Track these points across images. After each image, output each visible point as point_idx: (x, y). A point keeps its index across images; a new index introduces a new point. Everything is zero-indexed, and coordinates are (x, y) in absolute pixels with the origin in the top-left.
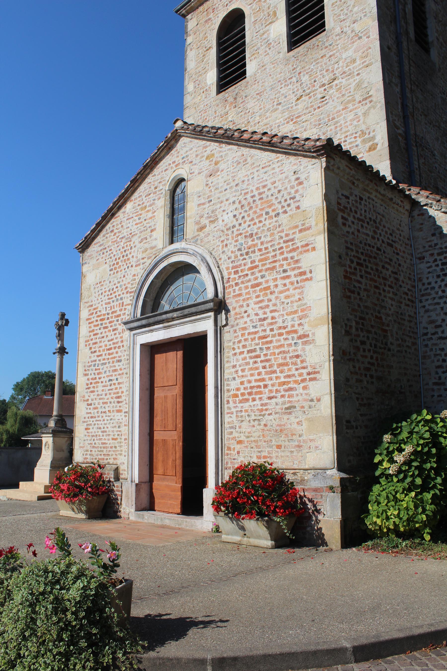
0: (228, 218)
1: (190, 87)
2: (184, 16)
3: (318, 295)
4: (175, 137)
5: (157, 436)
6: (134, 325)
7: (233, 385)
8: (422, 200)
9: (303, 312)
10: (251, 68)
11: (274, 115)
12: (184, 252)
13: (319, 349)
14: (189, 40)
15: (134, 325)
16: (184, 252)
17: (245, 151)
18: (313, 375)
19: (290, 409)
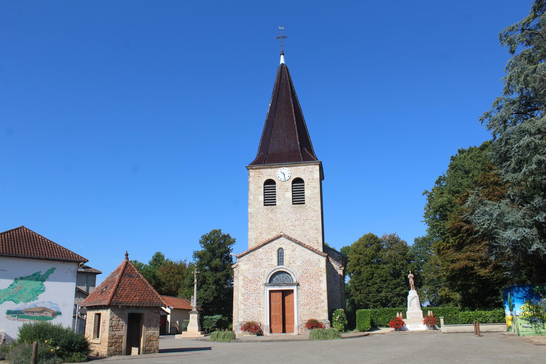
0: (299, 263)
1: (251, 197)
2: (248, 169)
3: (324, 286)
4: (281, 236)
5: (272, 314)
6: (266, 285)
7: (301, 303)
8: (330, 260)
9: (321, 289)
10: (278, 203)
11: (287, 222)
12: (283, 268)
13: (324, 296)
14: (250, 179)
15: (266, 285)
16: (283, 268)
17: (303, 248)
18: (323, 302)
19: (317, 308)
